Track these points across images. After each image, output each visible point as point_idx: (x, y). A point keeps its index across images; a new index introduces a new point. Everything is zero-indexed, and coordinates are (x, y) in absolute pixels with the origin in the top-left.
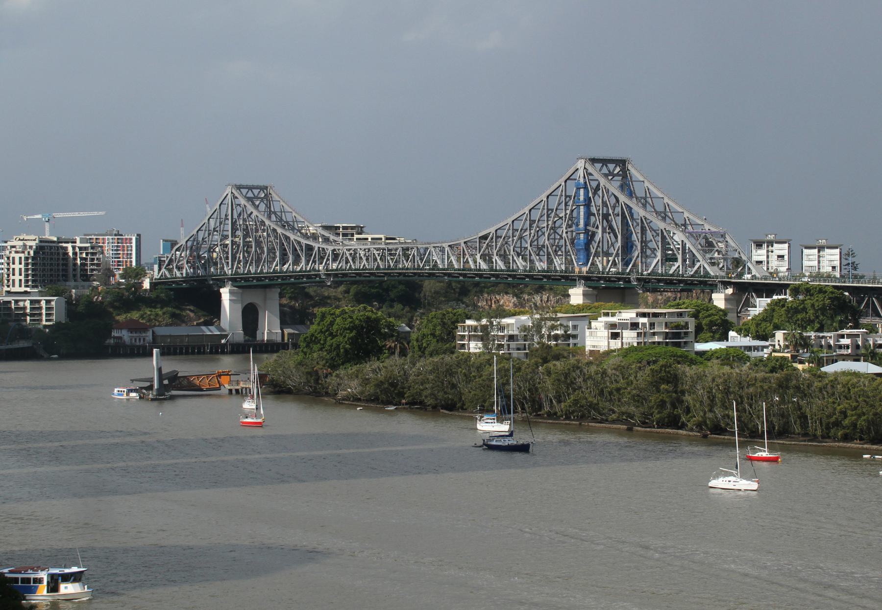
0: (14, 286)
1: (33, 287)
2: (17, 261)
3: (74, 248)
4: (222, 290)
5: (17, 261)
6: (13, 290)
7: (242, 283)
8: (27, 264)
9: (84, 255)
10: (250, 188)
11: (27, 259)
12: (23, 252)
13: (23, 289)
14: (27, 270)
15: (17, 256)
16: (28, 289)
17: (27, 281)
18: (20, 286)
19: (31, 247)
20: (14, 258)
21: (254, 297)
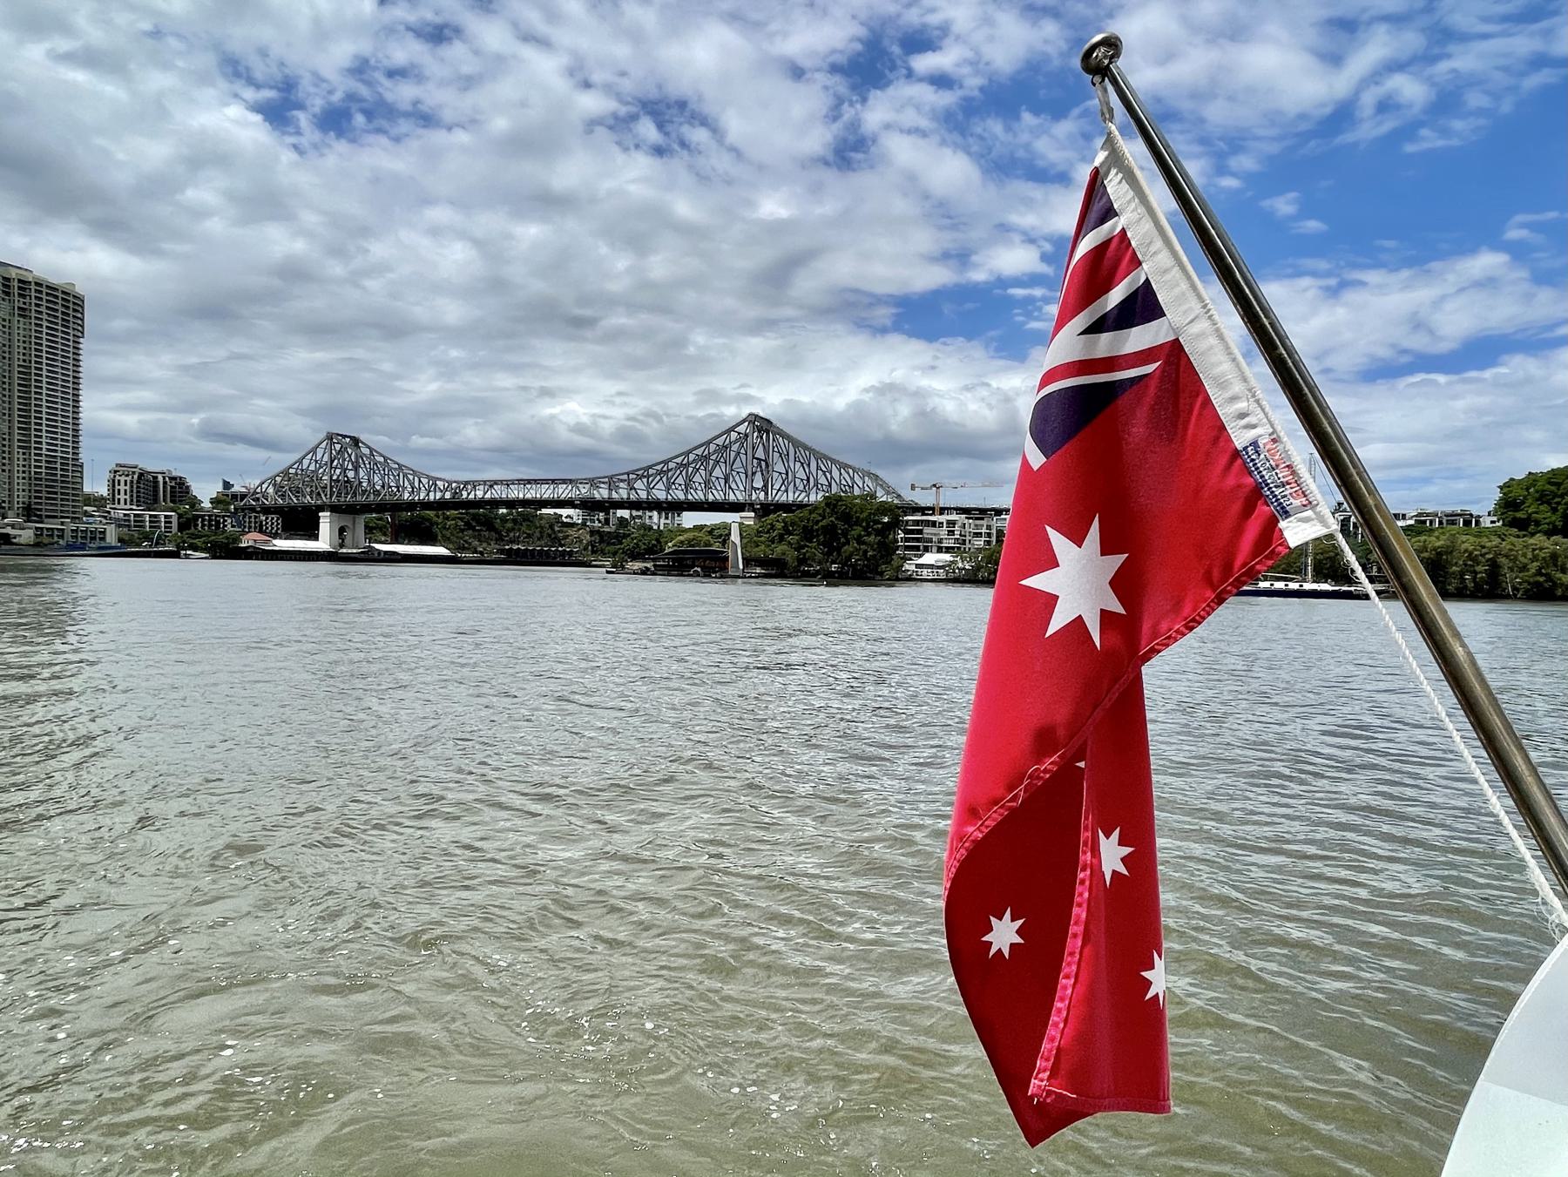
0: (119, 503)
1: (138, 506)
2: (122, 483)
3: (164, 478)
4: (320, 514)
5: (122, 483)
6: (119, 507)
7: (334, 509)
8: (132, 487)
9: (173, 484)
10: (344, 436)
11: (132, 482)
12: (127, 475)
13: (128, 507)
14: (132, 491)
15: (123, 479)
16: (134, 507)
17: (132, 500)
18: (126, 504)
19: (134, 473)
20: (119, 481)
21: (346, 520)
